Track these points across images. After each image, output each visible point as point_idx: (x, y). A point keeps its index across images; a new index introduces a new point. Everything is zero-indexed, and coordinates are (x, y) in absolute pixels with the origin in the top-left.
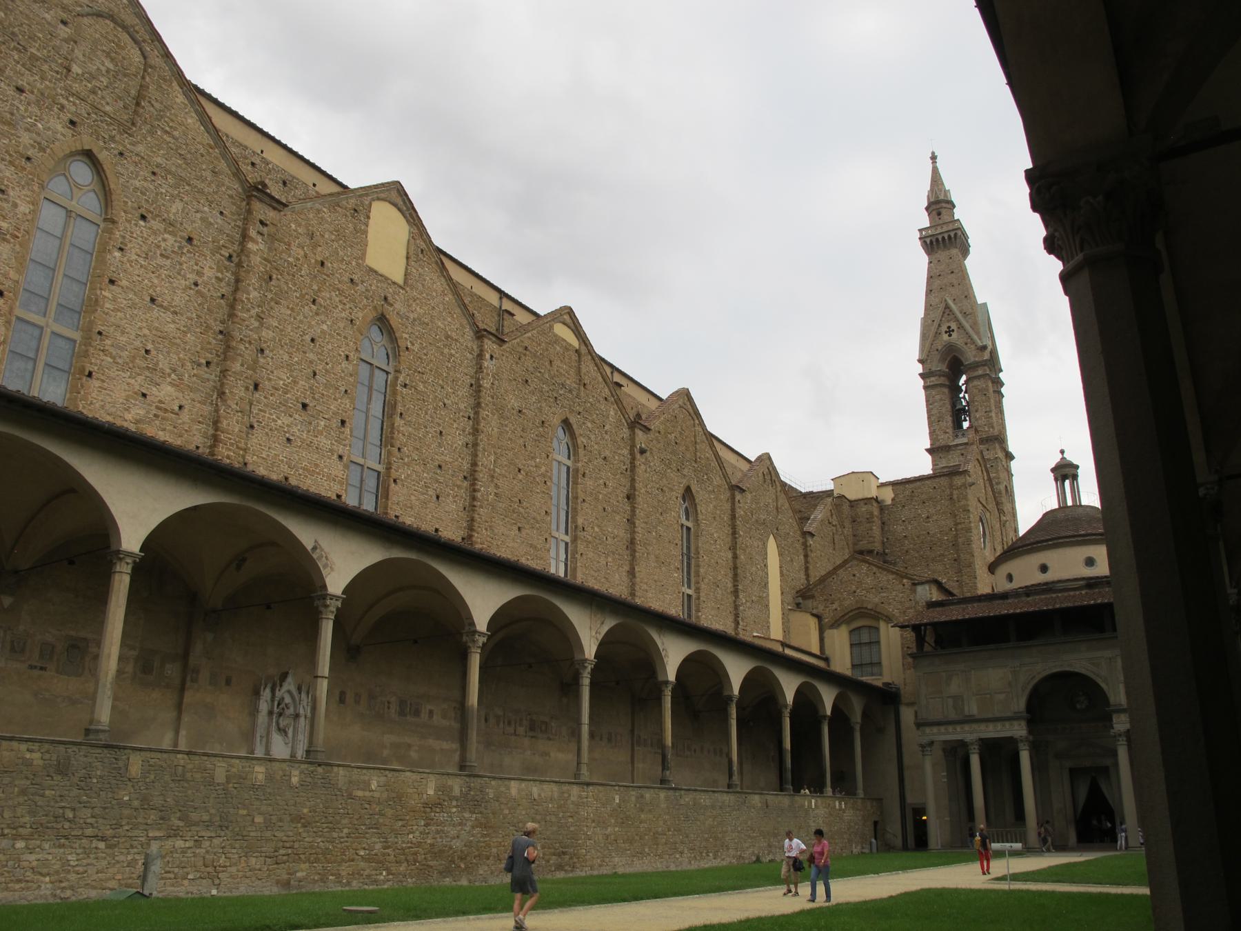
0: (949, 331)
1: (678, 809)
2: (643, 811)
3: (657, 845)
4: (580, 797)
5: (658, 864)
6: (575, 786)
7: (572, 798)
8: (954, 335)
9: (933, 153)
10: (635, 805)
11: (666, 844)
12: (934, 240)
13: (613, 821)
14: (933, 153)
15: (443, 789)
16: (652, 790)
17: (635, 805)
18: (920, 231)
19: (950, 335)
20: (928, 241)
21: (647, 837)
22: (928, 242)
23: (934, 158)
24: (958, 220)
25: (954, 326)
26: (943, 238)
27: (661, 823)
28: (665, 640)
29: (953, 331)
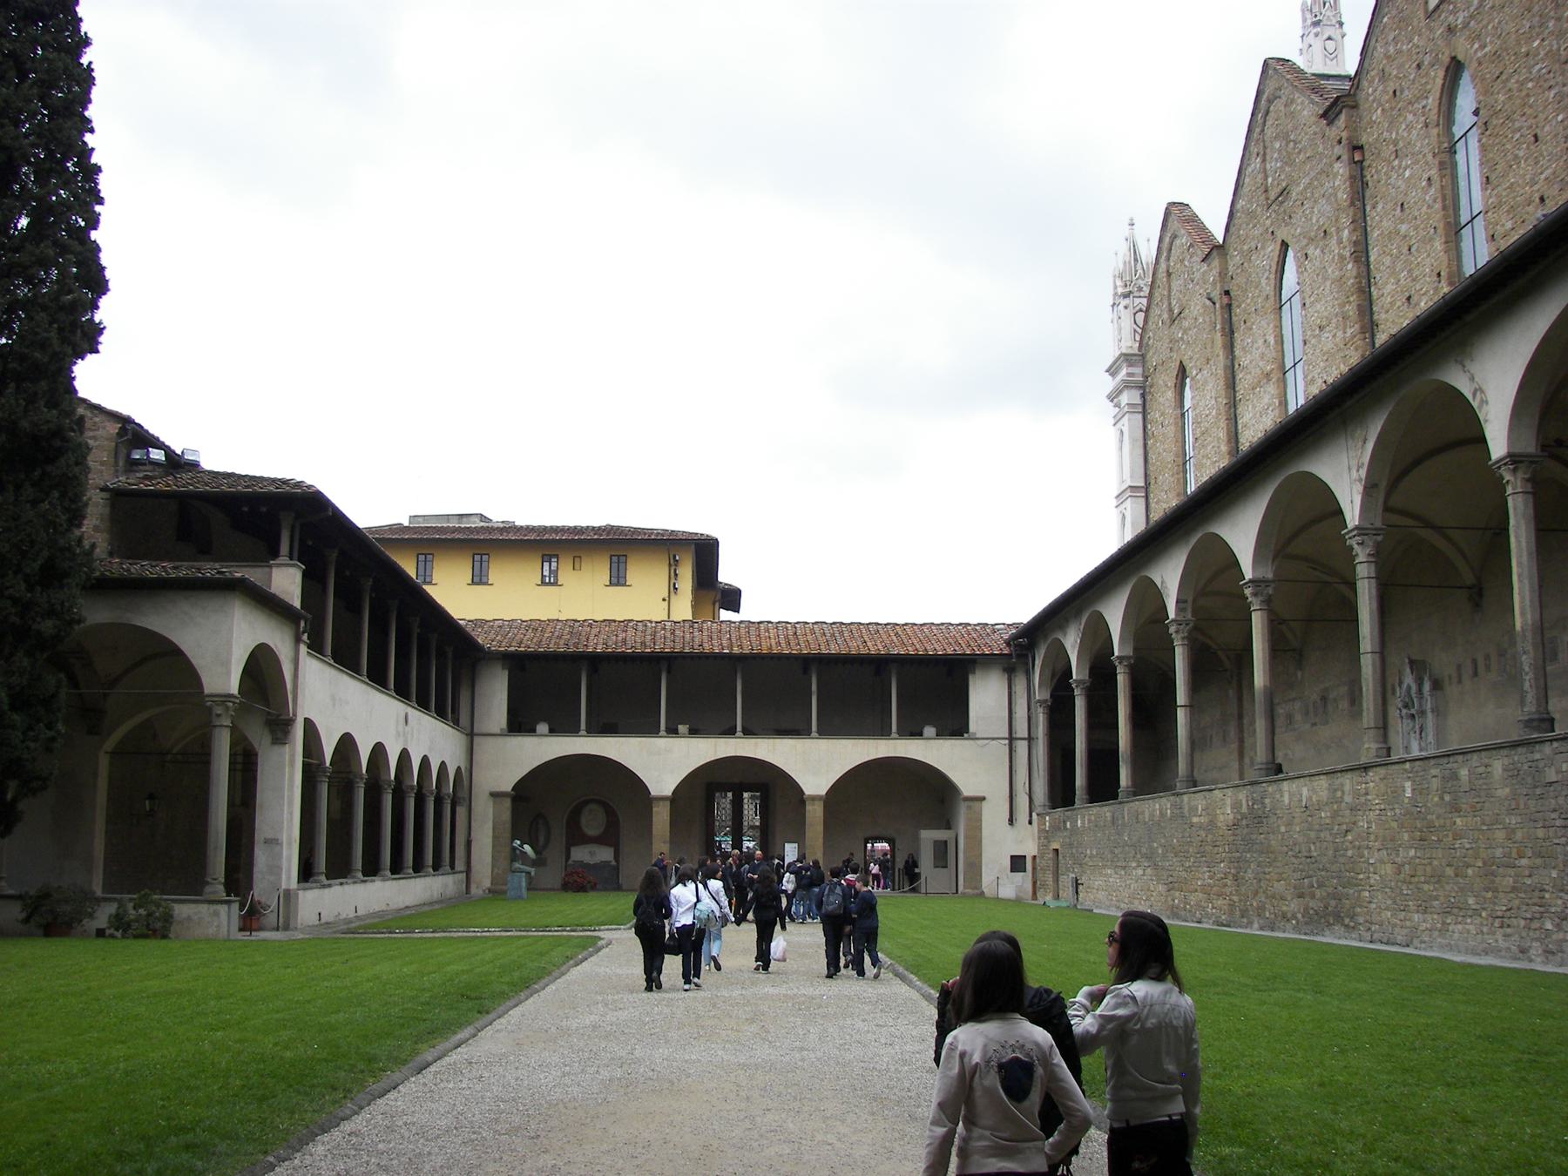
1: (1541, 797)
2: (1458, 810)
3: (1496, 891)
4: (1357, 794)
5: (1499, 936)
6: (1349, 775)
7: (1348, 799)
10: (1442, 798)
11: (1514, 889)
13: (1406, 836)
15: (1236, 806)
16: (1475, 756)
17: (1442, 798)
21: (1470, 871)
27: (1500, 835)
28: (1474, 367)
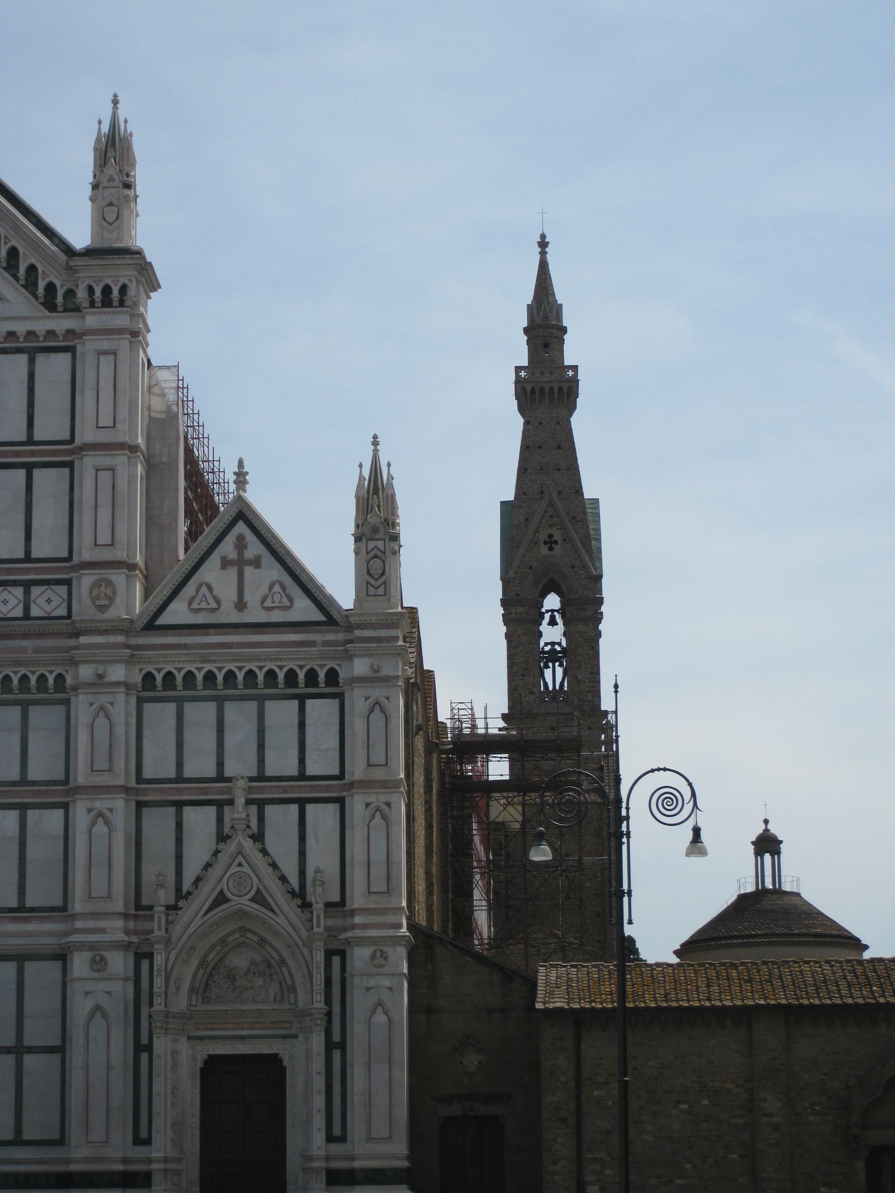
0: (551, 542)
8: (558, 549)
9: (543, 236)
12: (537, 390)
14: (543, 236)
18: (518, 369)
19: (551, 549)
20: (529, 388)
22: (529, 392)
23: (543, 244)
24: (575, 368)
25: (558, 536)
26: (551, 389)
29: (556, 542)
